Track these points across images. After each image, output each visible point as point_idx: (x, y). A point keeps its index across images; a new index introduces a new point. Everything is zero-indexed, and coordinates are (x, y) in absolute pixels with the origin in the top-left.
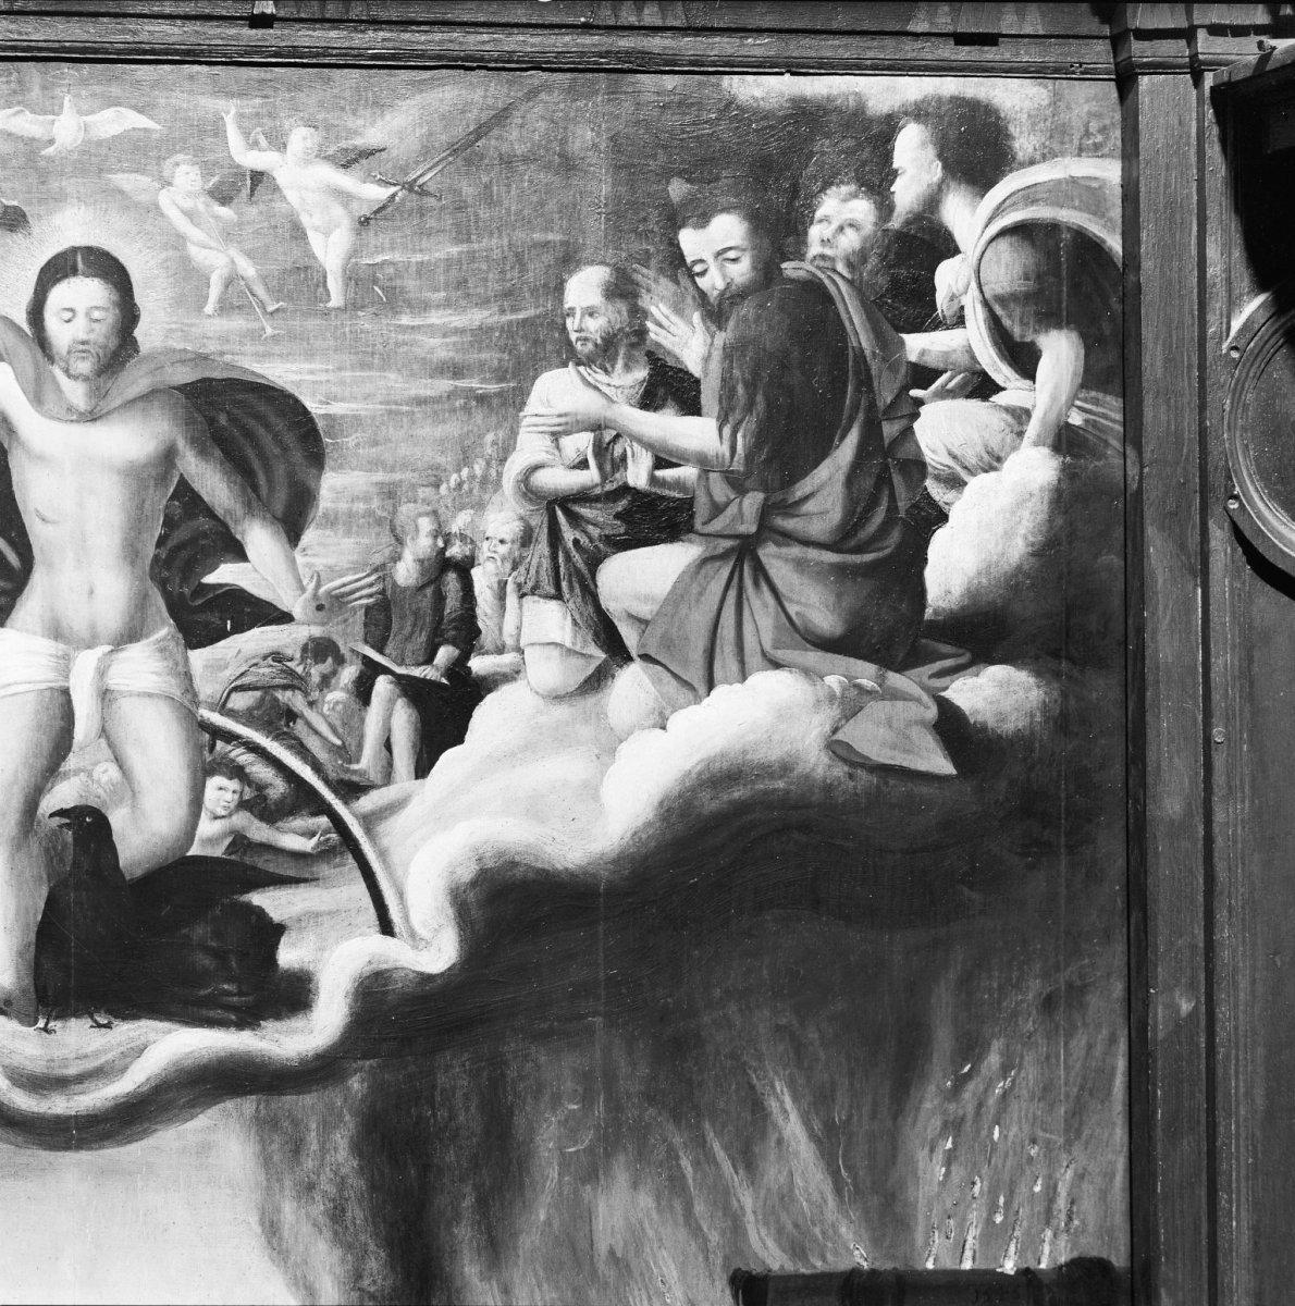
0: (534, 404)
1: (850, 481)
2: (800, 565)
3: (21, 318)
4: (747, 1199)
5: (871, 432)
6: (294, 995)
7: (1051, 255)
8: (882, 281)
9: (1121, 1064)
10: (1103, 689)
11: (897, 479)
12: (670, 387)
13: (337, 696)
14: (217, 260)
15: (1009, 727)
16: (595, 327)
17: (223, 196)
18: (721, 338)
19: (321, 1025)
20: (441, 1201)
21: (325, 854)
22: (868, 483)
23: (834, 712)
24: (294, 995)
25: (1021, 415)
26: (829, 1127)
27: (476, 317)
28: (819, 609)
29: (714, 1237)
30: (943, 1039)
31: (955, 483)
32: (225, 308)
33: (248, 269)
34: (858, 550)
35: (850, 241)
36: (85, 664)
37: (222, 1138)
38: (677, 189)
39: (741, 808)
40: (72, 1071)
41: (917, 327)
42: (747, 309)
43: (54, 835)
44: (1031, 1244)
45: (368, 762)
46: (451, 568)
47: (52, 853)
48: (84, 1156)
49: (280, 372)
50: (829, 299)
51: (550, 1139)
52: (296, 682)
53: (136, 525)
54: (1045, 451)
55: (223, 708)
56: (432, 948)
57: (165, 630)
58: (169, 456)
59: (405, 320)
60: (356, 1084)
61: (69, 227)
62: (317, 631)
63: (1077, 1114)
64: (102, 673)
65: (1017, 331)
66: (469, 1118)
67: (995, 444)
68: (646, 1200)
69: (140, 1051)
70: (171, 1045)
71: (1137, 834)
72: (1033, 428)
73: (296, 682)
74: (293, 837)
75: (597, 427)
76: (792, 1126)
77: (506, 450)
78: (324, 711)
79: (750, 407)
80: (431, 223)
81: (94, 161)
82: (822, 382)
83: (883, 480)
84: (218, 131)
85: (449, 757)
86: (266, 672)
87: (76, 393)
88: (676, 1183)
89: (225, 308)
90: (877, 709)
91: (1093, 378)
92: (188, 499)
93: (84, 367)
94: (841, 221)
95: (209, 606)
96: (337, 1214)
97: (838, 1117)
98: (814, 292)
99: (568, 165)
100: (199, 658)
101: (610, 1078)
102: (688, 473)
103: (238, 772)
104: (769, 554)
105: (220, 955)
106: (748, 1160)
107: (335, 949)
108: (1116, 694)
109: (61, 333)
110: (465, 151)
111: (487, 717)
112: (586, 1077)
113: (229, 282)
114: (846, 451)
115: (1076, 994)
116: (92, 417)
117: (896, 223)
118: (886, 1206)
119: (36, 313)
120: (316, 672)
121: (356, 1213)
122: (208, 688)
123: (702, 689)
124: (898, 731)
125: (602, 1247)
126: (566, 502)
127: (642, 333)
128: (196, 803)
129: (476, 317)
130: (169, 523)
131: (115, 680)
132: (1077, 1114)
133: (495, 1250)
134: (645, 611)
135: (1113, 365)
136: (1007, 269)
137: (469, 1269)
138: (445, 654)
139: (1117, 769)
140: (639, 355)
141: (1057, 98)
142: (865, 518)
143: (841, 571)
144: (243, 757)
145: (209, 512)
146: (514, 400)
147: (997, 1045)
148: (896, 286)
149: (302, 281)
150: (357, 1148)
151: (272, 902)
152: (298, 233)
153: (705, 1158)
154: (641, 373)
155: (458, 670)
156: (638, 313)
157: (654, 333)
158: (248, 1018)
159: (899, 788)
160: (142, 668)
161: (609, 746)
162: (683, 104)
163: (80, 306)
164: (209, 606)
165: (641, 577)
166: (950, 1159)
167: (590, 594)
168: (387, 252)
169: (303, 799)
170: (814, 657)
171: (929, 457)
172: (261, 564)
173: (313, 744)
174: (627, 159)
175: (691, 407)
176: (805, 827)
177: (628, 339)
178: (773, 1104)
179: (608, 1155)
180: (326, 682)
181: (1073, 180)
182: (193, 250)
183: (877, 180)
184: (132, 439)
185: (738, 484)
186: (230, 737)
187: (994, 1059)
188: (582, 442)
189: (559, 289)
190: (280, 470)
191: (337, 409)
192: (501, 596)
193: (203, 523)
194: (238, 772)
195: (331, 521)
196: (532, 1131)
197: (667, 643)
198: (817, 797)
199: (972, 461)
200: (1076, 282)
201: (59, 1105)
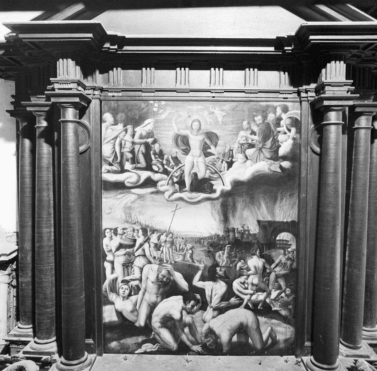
0: (239, 135)
1: (271, 142)
2: (266, 151)
3: (190, 126)
4: (259, 213)
5: (274, 137)
6: (214, 191)
7: (293, 120)
8: (275, 123)
9: (297, 201)
10: (297, 164)
11: (276, 142)
12: (253, 133)
13: (220, 162)
14: (209, 120)
15: (287, 167)
16: (246, 127)
17: (209, 114)
18: (259, 128)
19: (217, 194)
20: (228, 212)
21: (218, 178)
22: (273, 143)
23: (269, 165)
24: (214, 191)
25: (289, 136)
26: (267, 206)
27: (234, 126)
29: (255, 217)
30: (279, 198)
31: (282, 143)
32: (210, 125)
33: (212, 121)
34: (272, 149)
35: (272, 119)
36: (196, 159)
37: (208, 204)
38: (254, 113)
39: (259, 175)
40: (193, 197)
41: (278, 127)
42: (261, 125)
43: (192, 175)
44: (288, 219)
45: (222, 169)
47: (192, 177)
48: (194, 206)
49: (215, 131)
50: (269, 124)
51: (239, 206)
52: (216, 161)
53: (201, 146)
54: (292, 140)
55: (208, 163)
56: (228, 187)
57: (203, 156)
58: (204, 139)
59: (227, 126)
60: (221, 200)
61: (195, 117)
62: (218, 156)
63: (293, 206)
64: (197, 160)
65: (289, 128)
66: (231, 204)
67: (286, 139)
68: (249, 213)
69: (200, 196)
70: (202, 195)
71: (300, 179)
72: (290, 137)
73: (216, 161)
74: (215, 176)
75: (246, 137)
76: (263, 205)
77: (237, 139)
78: (218, 164)
79: (261, 135)
80: (230, 117)
82: (269, 134)
83: (275, 142)
84: (209, 108)
85: (230, 169)
86: (213, 160)
87: (195, 133)
88: (252, 211)
89: (210, 125)
90: (273, 165)
91: (297, 133)
92: (206, 143)
93: (196, 131)
94: (271, 117)
95: (207, 154)
96: (218, 212)
97: (268, 205)
98: (268, 124)
99: (243, 111)
100: (206, 159)
101: (245, 201)
102: (255, 141)
103: (210, 170)
104: (263, 149)
105: (208, 187)
106: (259, 209)
107: (219, 187)
108: (298, 165)
109: (194, 127)
110: (233, 110)
111: (234, 165)
112: (243, 200)
113: (210, 122)
114: (271, 139)
115: (293, 194)
116: (197, 135)
117: (277, 117)
118: (273, 214)
119: (192, 126)
120: (218, 160)
121: (220, 212)
122: (207, 161)
123: (255, 162)
124: (275, 167)
125: (244, 217)
126: (243, 144)
127: (250, 128)
128: (206, 173)
129: (234, 126)
130: (204, 145)
131: (198, 161)
132: (293, 206)
133: (234, 216)
134: (250, 155)
135: (299, 131)
136: (288, 121)
137: (231, 218)
138: (230, 159)
139: (298, 172)
140: (250, 130)
141: (294, 104)
142: (272, 146)
143: (270, 151)
144: (210, 168)
145: (208, 145)
146: (238, 134)
147: (285, 199)
148: (277, 123)
149: (217, 122)
150: (220, 206)
151: (212, 182)
152: (217, 118)
153: (255, 209)
154: (250, 131)
155: (231, 161)
156: (250, 125)
157: (252, 128)
158: (210, 193)
159: (275, 173)
160: (201, 159)
161: (246, 168)
162: (255, 105)
163: (196, 125)
164: (207, 154)
165: (250, 152)
166: (279, 210)
167: (245, 153)
168: (225, 120)
169: (216, 172)
170: (267, 160)
171: (279, 140)
172: (212, 150)
173: (217, 167)
174: (249, 110)
175: (255, 135)
176: (266, 177)
178: (262, 204)
179: (245, 208)
180: (218, 161)
181: (295, 113)
182: (207, 120)
183: (275, 113)
184: (201, 137)
185: (260, 143)
186: (209, 166)
187: (284, 200)
188: (244, 138)
189: (242, 123)
190: (215, 141)
191: (220, 135)
192: (236, 153)
193: (207, 146)
194: (210, 170)
195: (219, 146)
196: (237, 206)
197: (252, 158)
198: (267, 174)
199: (284, 141)
200: (296, 123)
201: (192, 201)
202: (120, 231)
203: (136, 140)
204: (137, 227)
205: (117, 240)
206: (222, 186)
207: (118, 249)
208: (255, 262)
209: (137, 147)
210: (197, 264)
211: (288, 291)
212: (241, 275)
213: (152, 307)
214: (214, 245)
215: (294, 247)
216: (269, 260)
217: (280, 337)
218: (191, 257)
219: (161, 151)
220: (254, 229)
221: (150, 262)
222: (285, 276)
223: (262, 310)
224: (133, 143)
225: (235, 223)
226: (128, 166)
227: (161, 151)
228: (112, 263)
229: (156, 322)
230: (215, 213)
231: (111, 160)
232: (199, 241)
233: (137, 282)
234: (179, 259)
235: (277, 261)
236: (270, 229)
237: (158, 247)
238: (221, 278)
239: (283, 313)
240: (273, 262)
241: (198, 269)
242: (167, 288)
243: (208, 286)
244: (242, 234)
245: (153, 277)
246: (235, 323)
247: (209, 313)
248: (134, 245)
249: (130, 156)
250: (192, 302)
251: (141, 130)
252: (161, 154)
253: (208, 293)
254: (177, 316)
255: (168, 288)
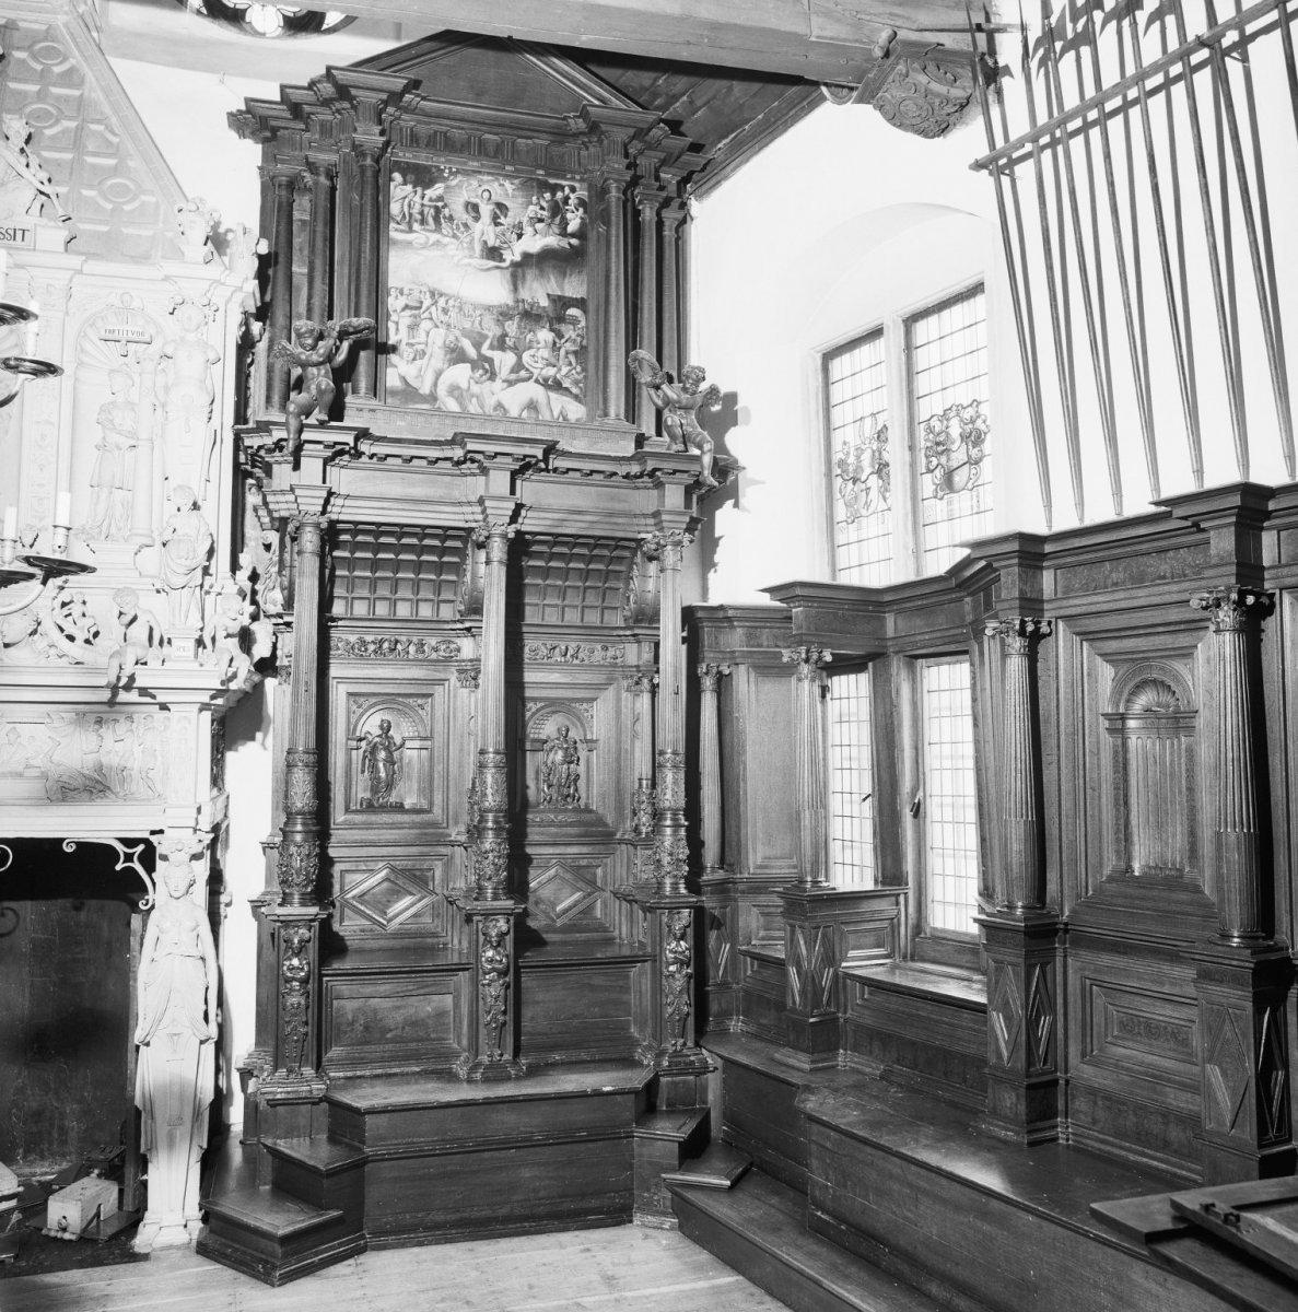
6: (504, 261)
12: (542, 208)
19: (507, 263)
24: (504, 261)
28: (557, 231)
37: (497, 271)
46: (520, 223)
61: (486, 187)
70: (492, 264)
81: (488, 181)
82: (557, 210)
118: (562, 290)
124: (564, 243)
137: (520, 287)
163: (486, 195)
165: (539, 226)
172: (502, 220)
177: (538, 203)
202: (406, 291)
203: (426, 201)
204: (424, 289)
205: (402, 301)
206: (513, 254)
207: (403, 310)
208: (545, 335)
209: (426, 210)
210: (485, 332)
211: (579, 369)
212: (530, 348)
213: (439, 374)
214: (504, 315)
215: (583, 324)
216: (560, 335)
217: (572, 417)
218: (480, 324)
219: (451, 216)
220: (544, 302)
221: (437, 326)
222: (575, 353)
223: (556, 386)
224: (423, 205)
225: (524, 294)
226: (416, 226)
227: (451, 216)
228: (397, 323)
229: (442, 392)
230: (505, 282)
231: (399, 219)
232: (489, 308)
233: (422, 347)
234: (468, 325)
235: (567, 337)
236: (561, 303)
237: (445, 311)
238: (510, 348)
239: (575, 390)
240: (563, 337)
241: (486, 337)
242: (454, 355)
243: (496, 355)
244: (532, 306)
245: (440, 343)
246: (525, 400)
247: (498, 384)
248: (420, 308)
249: (419, 217)
250: (481, 372)
251: (430, 193)
252: (451, 219)
253: (497, 363)
254: (464, 385)
255: (456, 356)
